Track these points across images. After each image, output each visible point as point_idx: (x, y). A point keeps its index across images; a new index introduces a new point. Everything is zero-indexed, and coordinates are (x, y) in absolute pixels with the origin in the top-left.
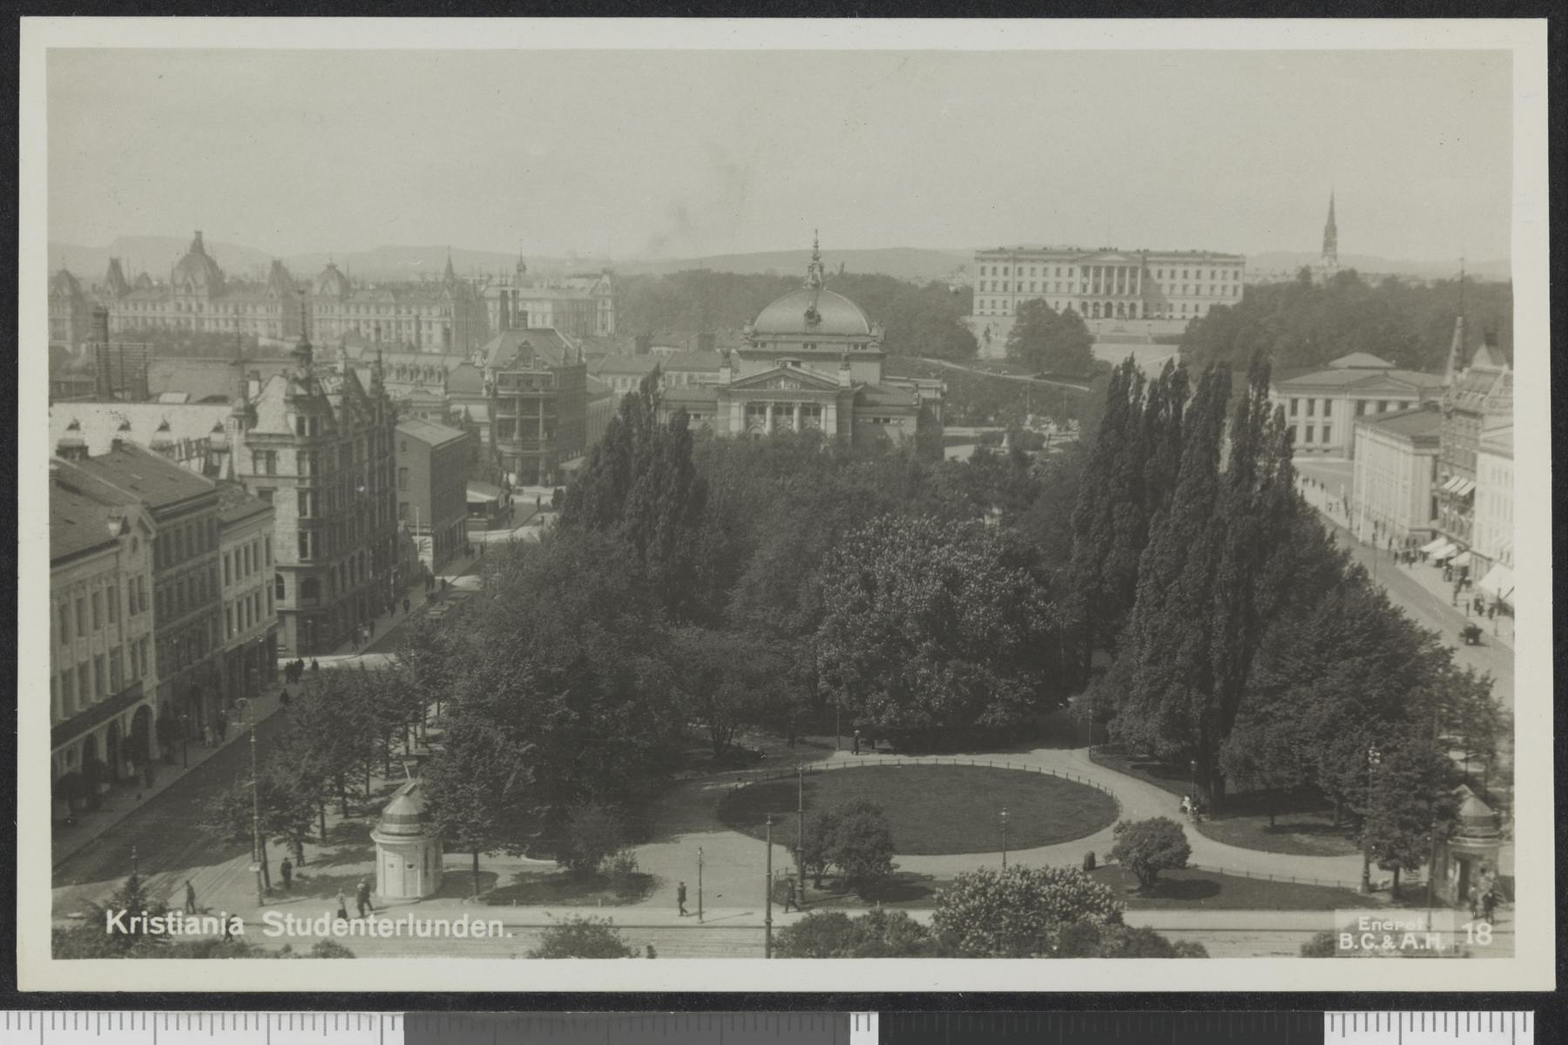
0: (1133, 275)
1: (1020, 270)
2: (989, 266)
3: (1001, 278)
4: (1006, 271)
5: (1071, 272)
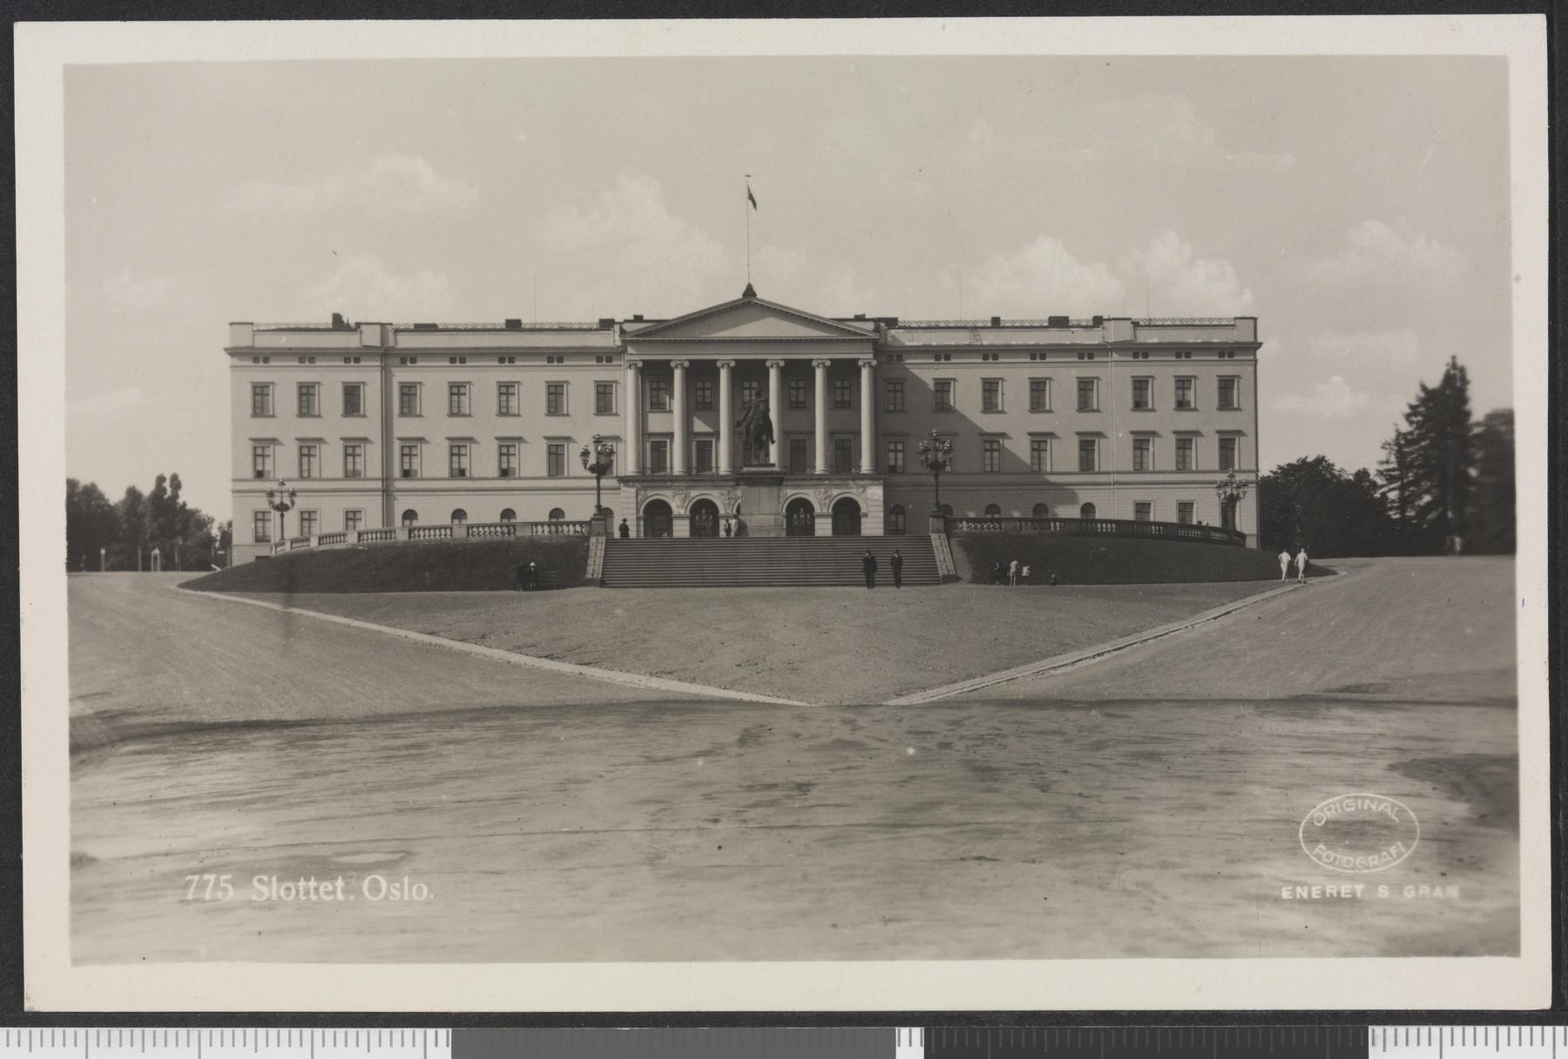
0: (843, 401)
1: (409, 391)
2: (285, 380)
3: (332, 424)
4: (352, 398)
5: (604, 399)
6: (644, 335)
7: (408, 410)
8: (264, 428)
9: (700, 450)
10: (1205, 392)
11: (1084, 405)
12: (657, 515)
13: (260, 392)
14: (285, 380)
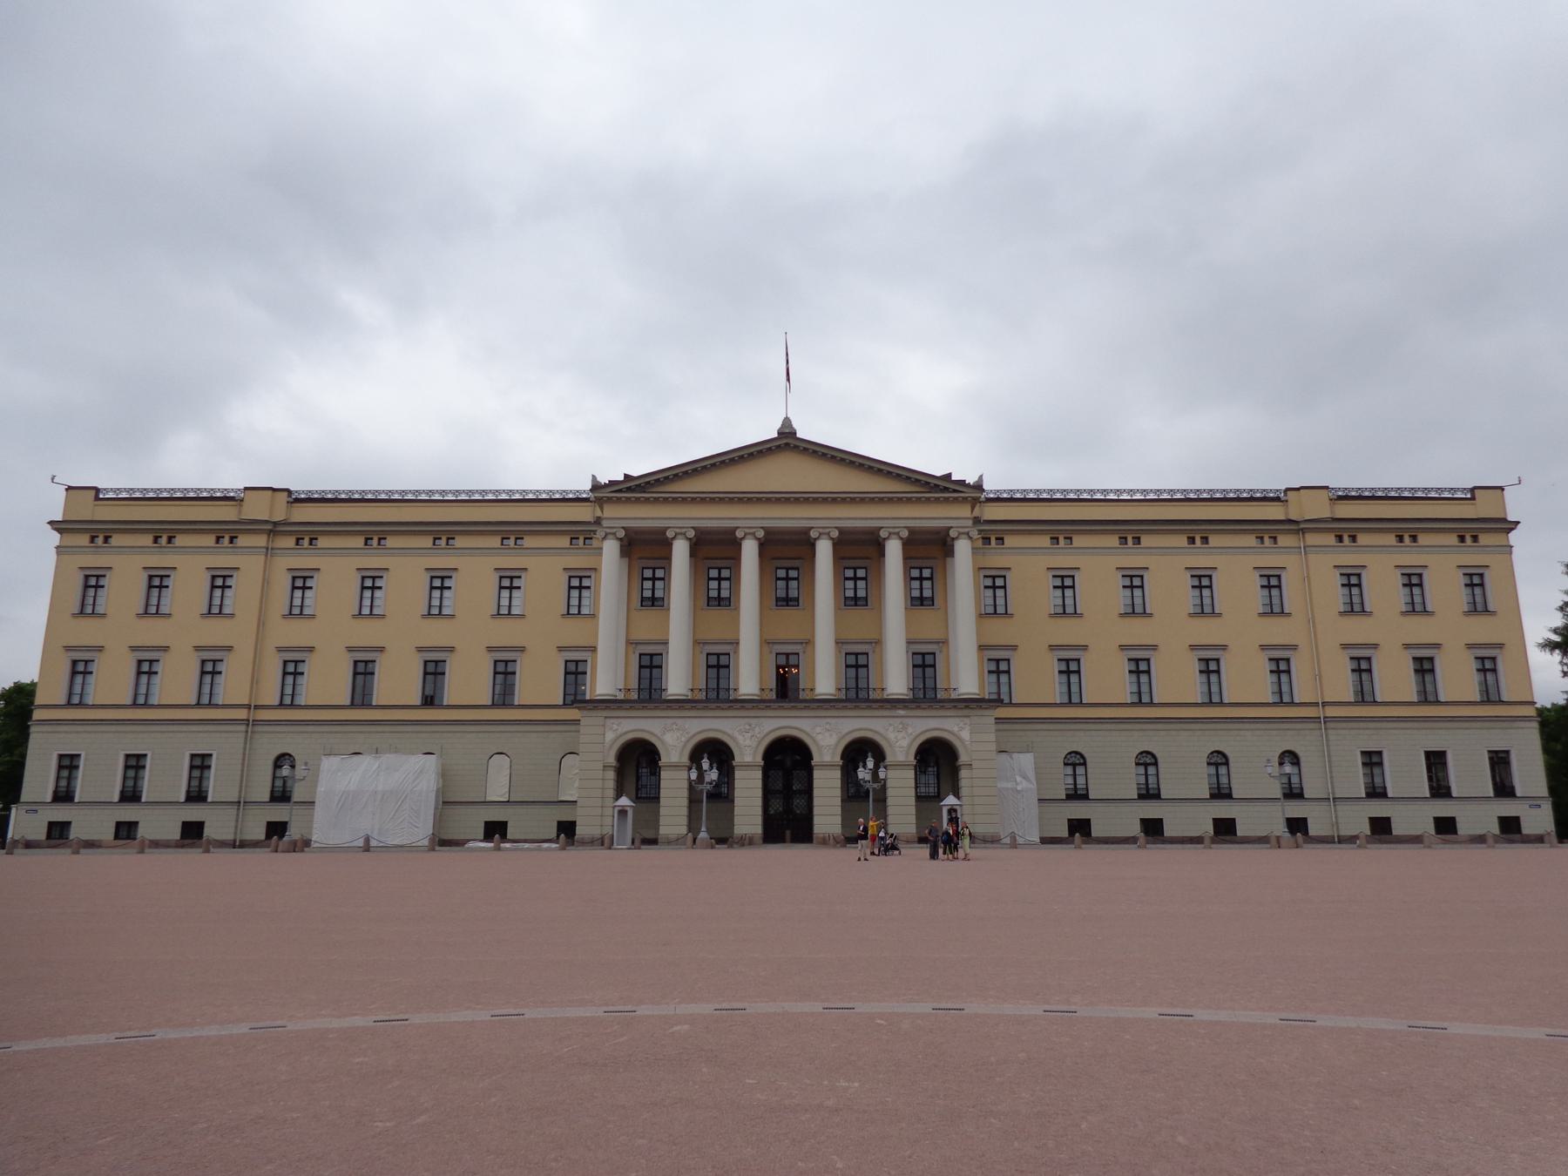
1: (301, 582)
6: (629, 489)
7: (296, 613)
8: (86, 632)
9: (718, 665)
10: (1444, 587)
11: (1275, 610)
12: (638, 762)
13: (93, 582)
14: (126, 571)
